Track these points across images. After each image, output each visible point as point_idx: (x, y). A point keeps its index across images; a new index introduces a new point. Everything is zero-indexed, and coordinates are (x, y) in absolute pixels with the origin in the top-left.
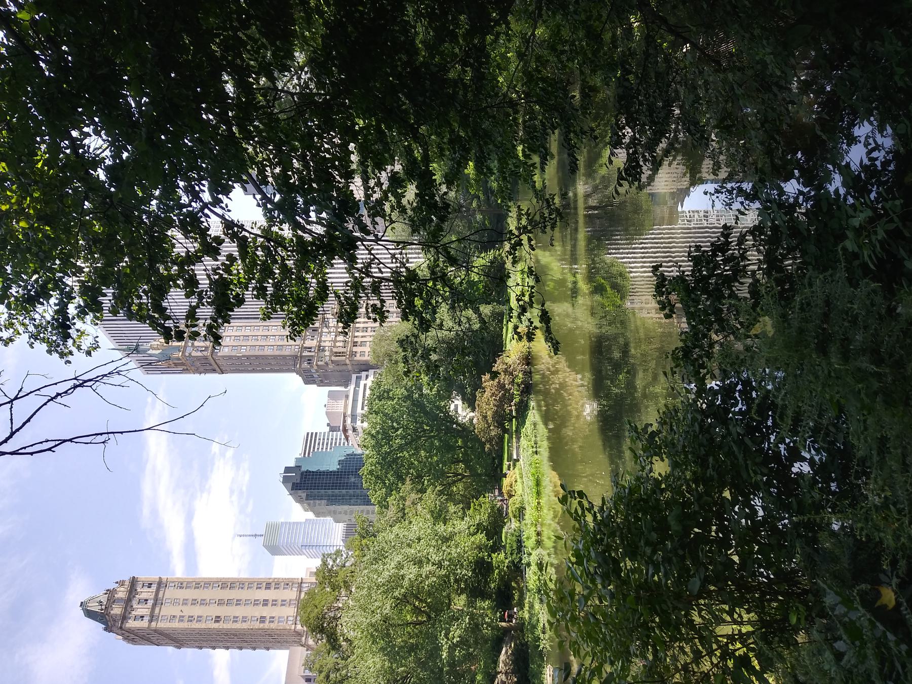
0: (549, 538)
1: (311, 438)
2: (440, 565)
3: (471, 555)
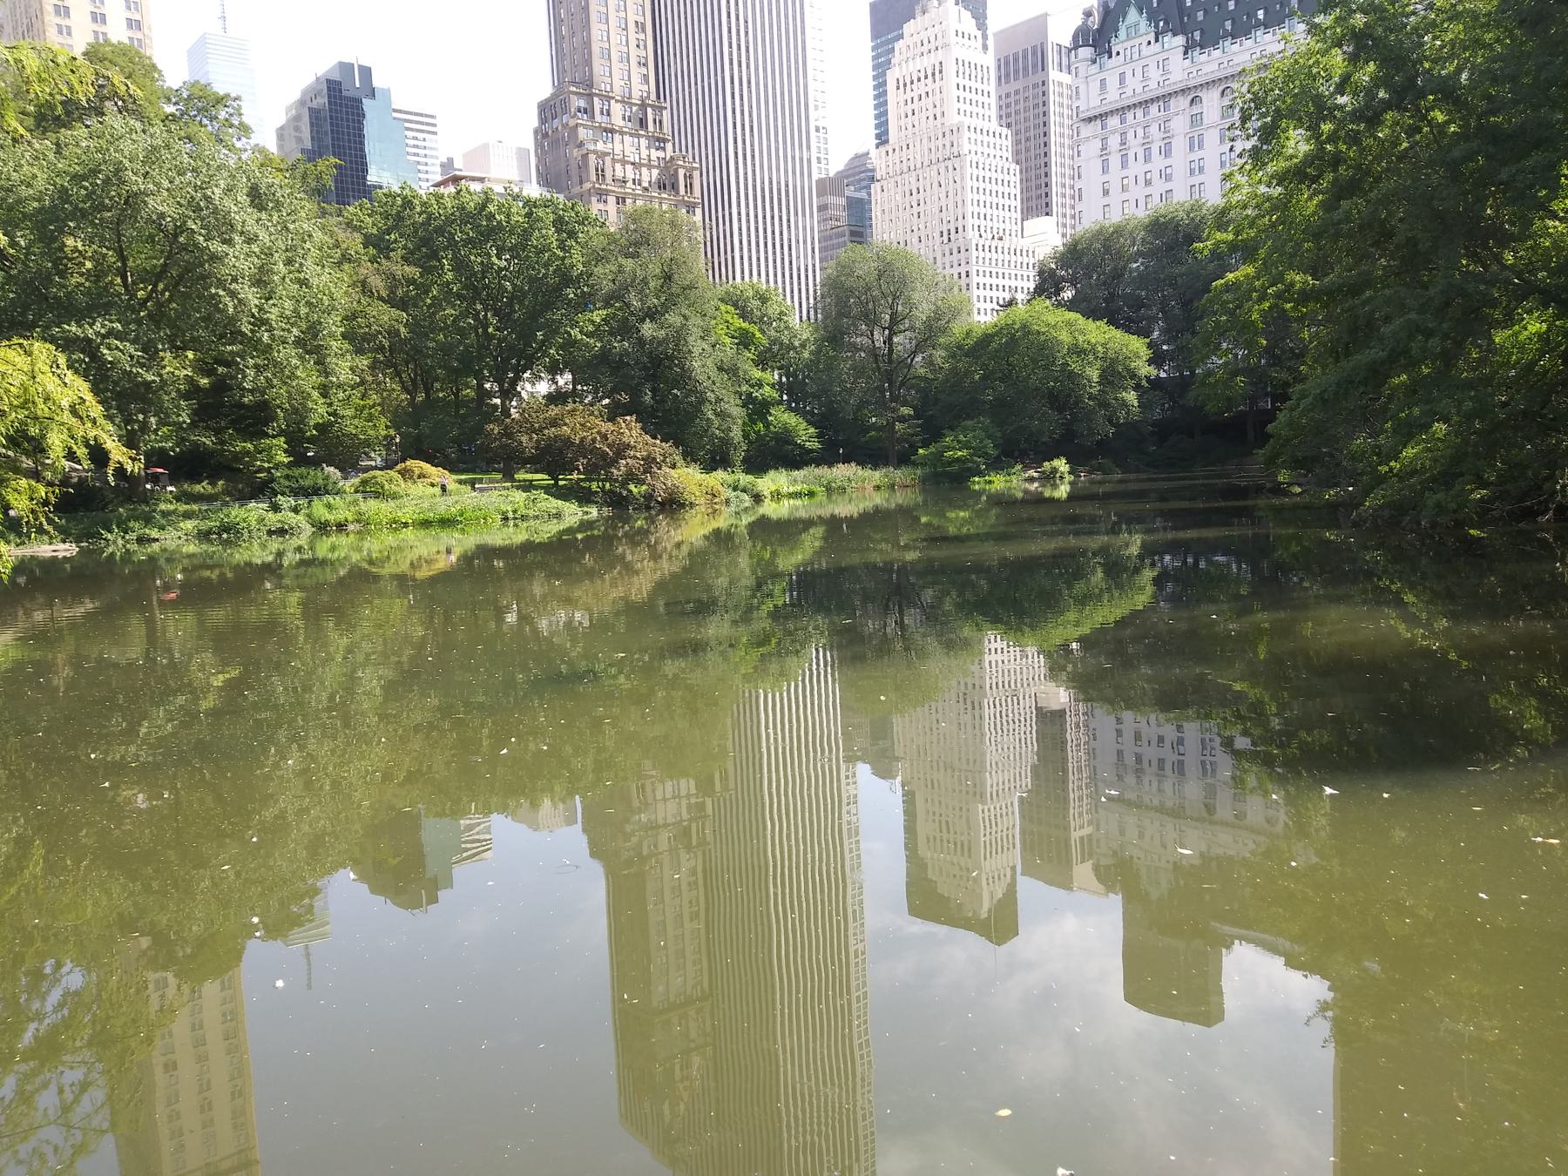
0: (333, 549)
1: (425, 123)
2: (260, 322)
3: (279, 394)
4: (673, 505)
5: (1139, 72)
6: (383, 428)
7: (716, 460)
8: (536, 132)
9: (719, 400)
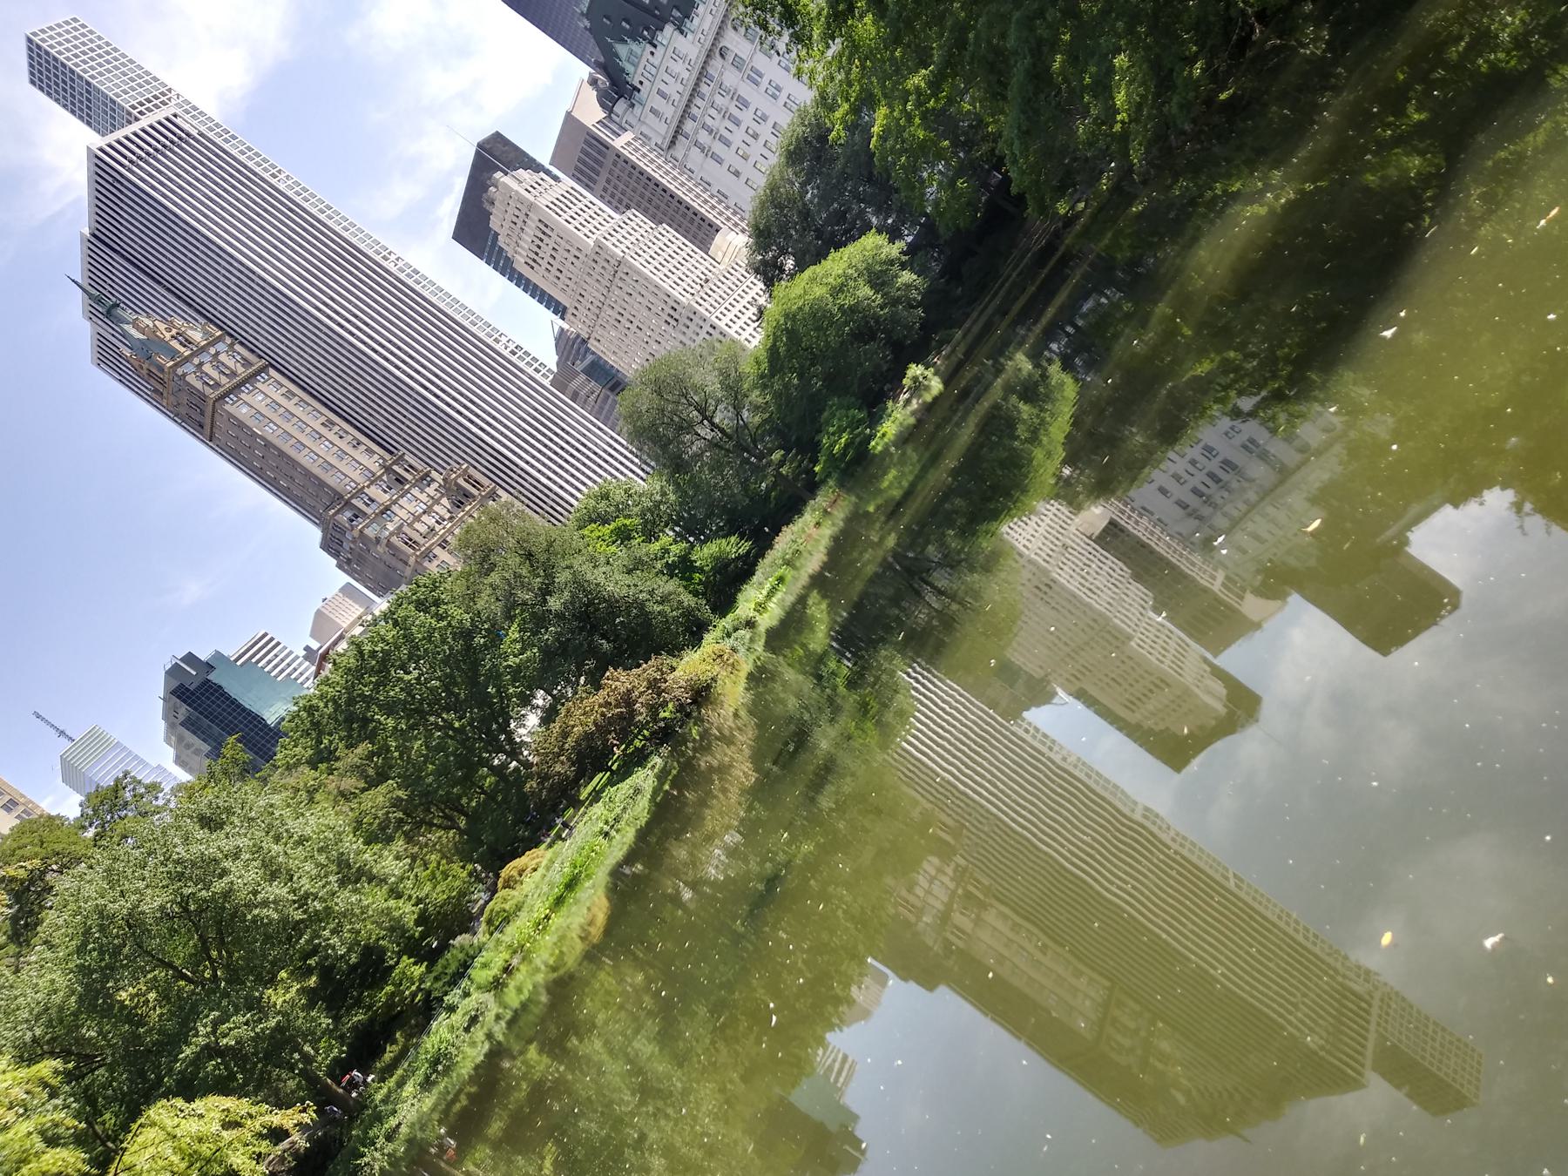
0: (519, 990)
1: (265, 643)
2: (302, 901)
3: (370, 931)
4: (702, 694)
5: (667, 78)
6: (460, 872)
7: (694, 631)
8: (339, 566)
9: (651, 593)
